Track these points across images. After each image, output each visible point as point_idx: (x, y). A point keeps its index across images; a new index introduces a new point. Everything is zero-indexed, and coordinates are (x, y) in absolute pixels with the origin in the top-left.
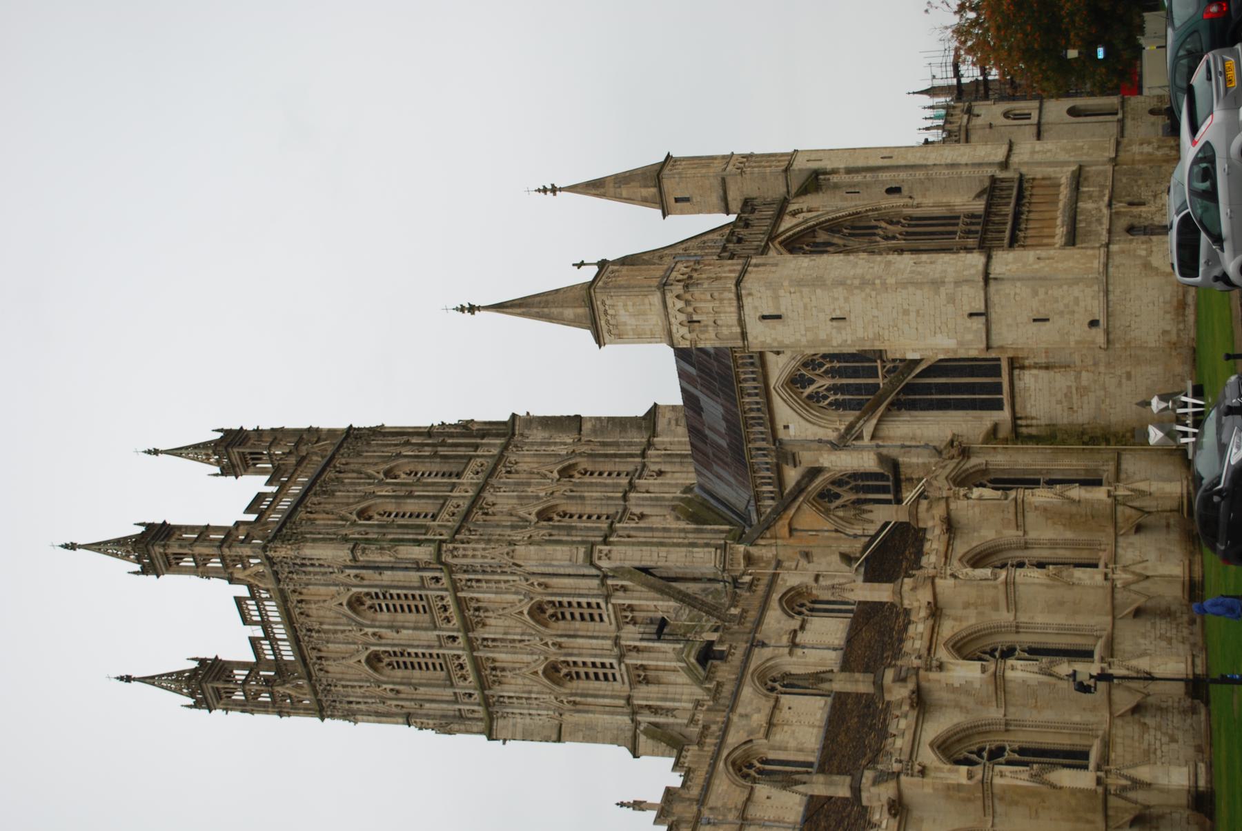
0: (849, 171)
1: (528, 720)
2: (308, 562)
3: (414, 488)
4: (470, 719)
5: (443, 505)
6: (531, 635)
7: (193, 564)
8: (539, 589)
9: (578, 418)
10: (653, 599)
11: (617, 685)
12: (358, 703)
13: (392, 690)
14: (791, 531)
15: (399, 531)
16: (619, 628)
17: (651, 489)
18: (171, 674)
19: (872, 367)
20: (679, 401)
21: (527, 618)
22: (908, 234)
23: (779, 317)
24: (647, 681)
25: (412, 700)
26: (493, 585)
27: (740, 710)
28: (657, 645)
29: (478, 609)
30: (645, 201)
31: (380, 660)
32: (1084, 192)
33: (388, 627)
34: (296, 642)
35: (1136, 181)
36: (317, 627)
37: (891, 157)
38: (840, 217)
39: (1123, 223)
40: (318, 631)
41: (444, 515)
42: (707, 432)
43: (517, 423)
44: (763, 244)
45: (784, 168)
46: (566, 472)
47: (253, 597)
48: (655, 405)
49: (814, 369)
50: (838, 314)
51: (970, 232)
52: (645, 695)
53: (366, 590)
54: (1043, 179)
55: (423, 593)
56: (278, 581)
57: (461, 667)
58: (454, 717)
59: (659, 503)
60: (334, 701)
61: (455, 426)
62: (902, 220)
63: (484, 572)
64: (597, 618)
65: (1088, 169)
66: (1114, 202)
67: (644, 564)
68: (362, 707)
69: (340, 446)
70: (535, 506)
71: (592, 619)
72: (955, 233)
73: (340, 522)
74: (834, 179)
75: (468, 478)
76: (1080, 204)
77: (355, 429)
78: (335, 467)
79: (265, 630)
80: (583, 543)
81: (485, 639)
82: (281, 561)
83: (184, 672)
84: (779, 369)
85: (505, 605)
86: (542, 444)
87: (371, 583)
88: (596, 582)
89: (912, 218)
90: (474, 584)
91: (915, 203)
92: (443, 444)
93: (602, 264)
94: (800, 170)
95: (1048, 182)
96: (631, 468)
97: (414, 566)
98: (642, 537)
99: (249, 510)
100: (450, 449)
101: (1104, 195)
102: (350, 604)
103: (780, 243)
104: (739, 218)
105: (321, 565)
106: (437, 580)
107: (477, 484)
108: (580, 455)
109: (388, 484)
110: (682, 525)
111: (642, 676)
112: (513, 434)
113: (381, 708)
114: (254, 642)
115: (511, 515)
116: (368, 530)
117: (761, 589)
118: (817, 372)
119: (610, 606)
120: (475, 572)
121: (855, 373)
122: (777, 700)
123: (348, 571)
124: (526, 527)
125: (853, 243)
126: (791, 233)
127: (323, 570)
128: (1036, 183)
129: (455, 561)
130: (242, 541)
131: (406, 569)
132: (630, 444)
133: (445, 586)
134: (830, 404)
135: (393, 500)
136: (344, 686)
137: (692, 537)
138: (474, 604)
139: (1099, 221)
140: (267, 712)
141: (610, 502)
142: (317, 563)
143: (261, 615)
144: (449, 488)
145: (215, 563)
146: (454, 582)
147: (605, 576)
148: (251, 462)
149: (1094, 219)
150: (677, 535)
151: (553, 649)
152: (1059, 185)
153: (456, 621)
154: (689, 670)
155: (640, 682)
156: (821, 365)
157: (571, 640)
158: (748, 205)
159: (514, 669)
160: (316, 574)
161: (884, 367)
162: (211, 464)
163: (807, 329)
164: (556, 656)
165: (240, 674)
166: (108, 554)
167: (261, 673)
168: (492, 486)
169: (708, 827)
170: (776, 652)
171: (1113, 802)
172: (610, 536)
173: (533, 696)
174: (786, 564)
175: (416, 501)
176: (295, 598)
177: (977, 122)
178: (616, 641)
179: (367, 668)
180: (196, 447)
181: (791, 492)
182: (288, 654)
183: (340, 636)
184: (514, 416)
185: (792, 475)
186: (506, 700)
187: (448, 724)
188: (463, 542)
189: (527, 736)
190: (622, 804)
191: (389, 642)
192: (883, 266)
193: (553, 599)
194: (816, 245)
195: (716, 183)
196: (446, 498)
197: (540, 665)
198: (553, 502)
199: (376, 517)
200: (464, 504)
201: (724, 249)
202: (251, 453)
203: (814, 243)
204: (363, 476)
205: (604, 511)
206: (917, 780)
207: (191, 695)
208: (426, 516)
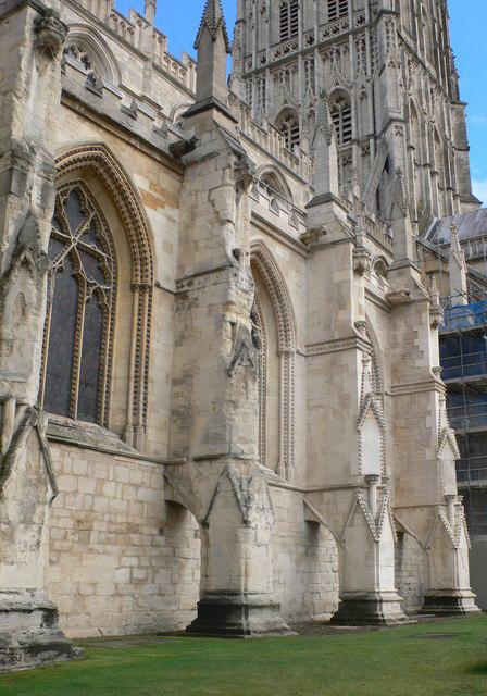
9: (467, 149)
13: (264, 8)
14: (430, 273)
21: (333, 89)
29: (338, 52)
81: (313, 61)
88: (371, 131)
106: (362, 20)
108: (445, 144)
132: (454, 183)
138: (342, 49)
147: (376, 138)
151: (307, 111)
159: (289, 87)
164: (303, 113)
171: (344, 499)
206: (352, 264)
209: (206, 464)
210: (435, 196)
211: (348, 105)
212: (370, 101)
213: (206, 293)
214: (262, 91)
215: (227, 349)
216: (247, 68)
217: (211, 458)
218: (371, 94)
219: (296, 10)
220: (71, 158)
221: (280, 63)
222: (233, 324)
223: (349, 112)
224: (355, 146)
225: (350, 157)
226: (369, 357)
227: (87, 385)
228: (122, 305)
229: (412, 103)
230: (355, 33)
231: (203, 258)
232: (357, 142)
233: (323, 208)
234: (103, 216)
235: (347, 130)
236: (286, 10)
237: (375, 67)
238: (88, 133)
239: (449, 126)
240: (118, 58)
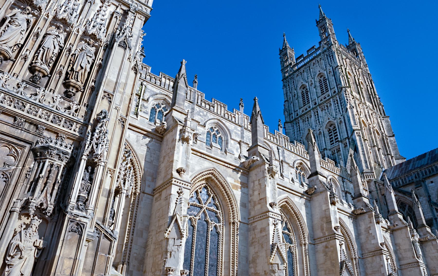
2: (331, 57)
8: (339, 121)
12: (289, 87)
13: (295, 94)
16: (330, 150)
21: (328, 121)
25: (293, 100)
26: (337, 107)
29: (327, 106)
31: (303, 89)
33: (315, 85)
34: (305, 65)
40: (309, 69)
42: (411, 164)
55: (329, 89)
56: (323, 53)
58: (290, 113)
59: (376, 157)
60: (288, 81)
63: (341, 103)
68: (288, 89)
81: (317, 112)
85: (330, 113)
87: (329, 76)
88: (346, 136)
105: (331, 61)
106: (335, 92)
108: (382, 135)
113: (288, 94)
114: (302, 55)
120: (340, 101)
131: (336, 83)
133: (333, 95)
136: (293, 82)
138: (329, 105)
142: (332, 59)
143: (311, 54)
147: (349, 139)
151: (318, 132)
157: (323, 136)
159: (309, 123)
160: (328, 61)
178: (326, 149)
179: (301, 85)
183: (309, 75)
185: (409, 189)
186: (298, 125)
187: (287, 112)
191: (310, 88)
207: (283, 49)
210: (381, 159)
211: (335, 127)
212: (344, 124)
214: (298, 127)
219: (308, 93)
220: (201, 175)
221: (304, 114)
223: (336, 130)
224: (340, 144)
225: (339, 148)
226: (343, 242)
227: (212, 266)
229: (363, 121)
230: (332, 97)
232: (341, 141)
233: (314, 178)
235: (336, 137)
236: (304, 93)
237: (344, 110)
238: (207, 165)
239: (383, 127)
240: (230, 128)
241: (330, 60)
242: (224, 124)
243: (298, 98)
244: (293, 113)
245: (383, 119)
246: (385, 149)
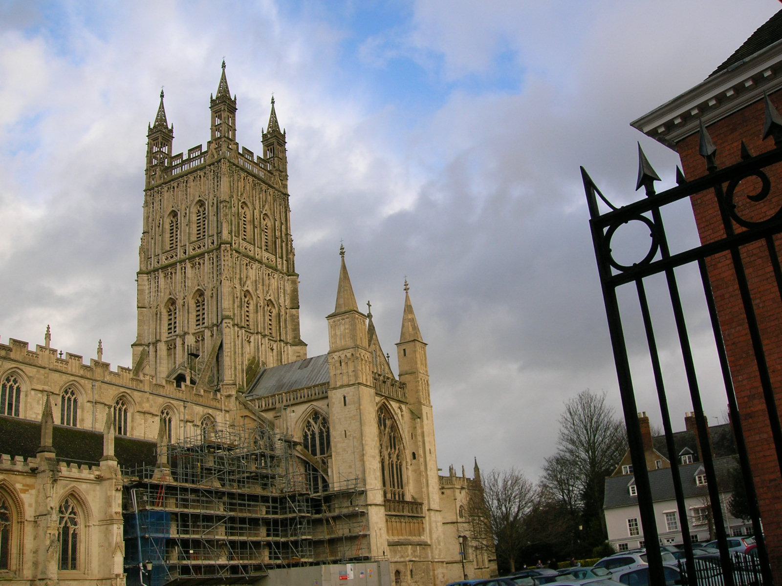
0: (423, 433)
1: (147, 292)
2: (219, 179)
3: (259, 229)
4: (147, 263)
5: (251, 244)
6: (188, 291)
7: (217, 124)
9: (298, 308)
10: (207, 351)
11: (166, 335)
12: (153, 207)
15: (236, 223)
16: (193, 334)
17: (263, 346)
18: (165, 116)
19: (324, 452)
20: (309, 357)
21: (196, 288)
22: (392, 465)
23: (345, 405)
24: (169, 349)
27: (151, 397)
28: (186, 353)
29: (199, 264)
30: (403, 334)
32: (416, 548)
33: (189, 220)
35: (423, 573)
36: (188, 185)
37: (430, 453)
38: (399, 431)
39: (401, 568)
41: (245, 244)
43: (294, 277)
44: (383, 394)
45: (422, 402)
46: (270, 303)
47: (201, 154)
48: (307, 345)
49: (322, 423)
50: (348, 434)
51: (395, 495)
52: (162, 347)
53: (206, 208)
54: (423, 528)
56: (210, 165)
57: (172, 257)
59: (256, 350)
61: (291, 246)
62: (399, 462)
64: (198, 323)
65: (429, 549)
66: (412, 563)
67: (224, 345)
69: (279, 191)
70: (252, 289)
71: (197, 321)
72: (394, 487)
73: (239, 194)
74: (418, 426)
75: (266, 255)
76: (410, 546)
77: (288, 198)
78: (268, 189)
79: (186, 160)
80: (234, 314)
82: (219, 166)
83: (166, 122)
84: (320, 405)
86: (284, 290)
88: (215, 322)
89: (401, 466)
90: (212, 261)
91: (408, 467)
92: (282, 241)
93: (370, 316)
94: (421, 410)
95: (421, 530)
96: (274, 335)
97: (219, 231)
98: (238, 342)
99: (244, 149)
100: (280, 245)
101: (415, 558)
102: (200, 201)
103: (384, 402)
104: (396, 381)
106: (213, 243)
107: (262, 260)
108: (279, 309)
109: (260, 216)
110: (246, 363)
111: (171, 347)
112: (288, 276)
113: (150, 219)
114: (181, 155)
115: (247, 278)
116: (236, 207)
117: (215, 404)
118: (321, 425)
119: (203, 329)
121: (322, 444)
122: (157, 415)
123: (215, 199)
124: (241, 285)
125: (386, 439)
126: (390, 407)
127: (216, 187)
128: (421, 524)
129: (222, 251)
130: (228, 147)
132: (286, 334)
134: (306, 432)
135: (252, 219)
137: (239, 367)
139: (402, 557)
140: (147, 163)
141: (256, 326)
143: (193, 158)
144: (259, 246)
145: (218, 134)
146: (212, 251)
147: (218, 326)
148: (269, 148)
149: (403, 554)
150: (240, 360)
152: (420, 536)
153: (193, 253)
154: (174, 370)
155: (168, 346)
156: (324, 427)
157: (186, 311)
158: (403, 386)
161: (325, 458)
162: (268, 129)
163: (340, 419)
164: (180, 302)
165: (165, 150)
166: (220, 83)
167: (166, 160)
168: (261, 267)
169: (91, 386)
170: (182, 414)
172: (238, 327)
173: (159, 294)
174: (227, 415)
175: (252, 230)
176: (202, 174)
177: (458, 491)
179: (170, 211)
180: (276, 122)
181: (262, 416)
182: (176, 172)
184: (298, 275)
186: (157, 280)
188: (231, 255)
189: (140, 292)
190: (100, 342)
192: (373, 454)
193: (206, 301)
194: (384, 420)
195: (414, 370)
196: (254, 245)
197: (174, 296)
198: (254, 298)
199: (243, 211)
200: (251, 254)
201: (379, 375)
202: (274, 148)
203: (385, 419)
204: (264, 203)
205: (251, 323)
208: (245, 235)
209: (42, 581)
213: (42, 522)
214: (157, 284)
215: (48, 542)
216: (149, 266)
217: (43, 579)
218: (217, 296)
222: (50, 534)
224: (206, 331)
228: (15, 528)
231: (42, 510)
234: (7, 499)
241: (216, 184)
242: (22, 370)
243: (162, 232)
244: (152, 258)
245: (288, 280)
246: (278, 332)
